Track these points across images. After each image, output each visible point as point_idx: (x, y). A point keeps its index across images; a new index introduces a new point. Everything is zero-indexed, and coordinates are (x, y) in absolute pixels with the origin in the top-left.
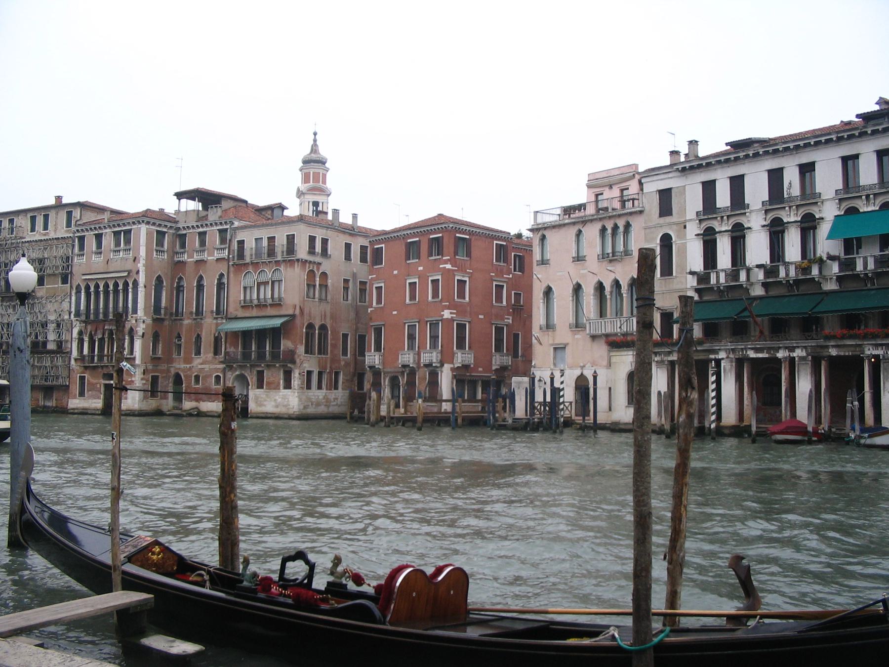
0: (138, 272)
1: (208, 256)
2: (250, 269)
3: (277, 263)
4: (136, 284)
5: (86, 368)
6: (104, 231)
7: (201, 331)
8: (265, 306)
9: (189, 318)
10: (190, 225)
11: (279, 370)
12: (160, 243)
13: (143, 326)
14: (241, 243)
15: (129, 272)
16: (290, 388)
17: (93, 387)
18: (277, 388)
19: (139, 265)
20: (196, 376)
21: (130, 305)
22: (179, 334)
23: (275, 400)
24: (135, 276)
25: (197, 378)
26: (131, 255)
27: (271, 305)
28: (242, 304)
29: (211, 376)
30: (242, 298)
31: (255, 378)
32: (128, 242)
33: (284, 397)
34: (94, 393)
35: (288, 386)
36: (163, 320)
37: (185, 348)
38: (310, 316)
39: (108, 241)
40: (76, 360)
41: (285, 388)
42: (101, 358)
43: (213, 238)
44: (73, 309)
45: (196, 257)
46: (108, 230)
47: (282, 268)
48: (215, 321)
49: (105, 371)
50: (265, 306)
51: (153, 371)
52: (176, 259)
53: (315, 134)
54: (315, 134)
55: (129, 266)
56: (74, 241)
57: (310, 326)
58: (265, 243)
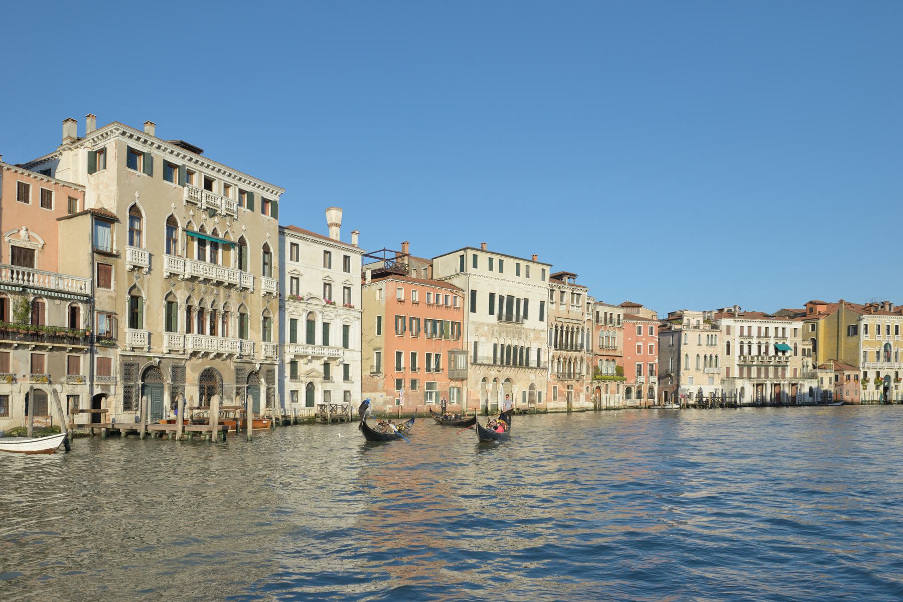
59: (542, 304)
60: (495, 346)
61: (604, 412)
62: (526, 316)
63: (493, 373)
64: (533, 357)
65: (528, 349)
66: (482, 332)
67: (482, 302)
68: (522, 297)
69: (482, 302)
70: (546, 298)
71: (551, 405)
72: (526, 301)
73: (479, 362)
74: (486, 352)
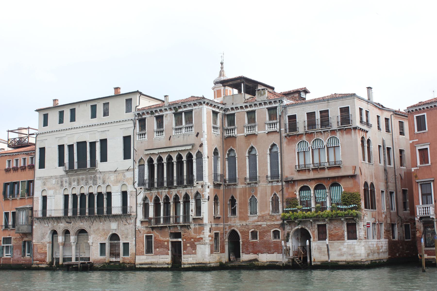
0: (201, 145)
1: (259, 130)
2: (304, 138)
3: (333, 132)
4: (200, 155)
5: (153, 228)
6: (164, 113)
7: (256, 194)
8: (323, 169)
9: (242, 183)
10: (239, 106)
11: (342, 222)
12: (215, 122)
13: (208, 190)
14: (292, 118)
15: (193, 145)
16: (355, 238)
17: (160, 244)
18: (341, 238)
19: (202, 139)
20: (252, 232)
21: (195, 173)
22: (233, 197)
23: (340, 250)
24: (199, 149)
25: (254, 234)
26: (194, 131)
27: (329, 168)
28: (298, 169)
30: (297, 164)
31: (316, 232)
32: (189, 120)
33: (350, 247)
34: (161, 250)
35: (352, 235)
36: (220, 185)
37: (240, 208)
38: (365, 176)
39: (169, 120)
40: (142, 222)
41: (349, 238)
42: (167, 219)
43: (262, 114)
44: (137, 180)
45: (246, 132)
46: (169, 112)
47: (338, 135)
48: (270, 185)
49: (173, 230)
50: (323, 169)
51: (217, 229)
52: (226, 135)
53: (222, 64)
54: (222, 64)
55: (192, 139)
56: (135, 124)
57: (366, 184)
58: (318, 116)
59: (127, 140)
60: (66, 197)
63: (61, 226)
64: (117, 202)
67: (52, 156)
68: (97, 138)
69: (52, 156)
70: (129, 129)
71: (142, 259)
73: (48, 215)
74: (55, 207)
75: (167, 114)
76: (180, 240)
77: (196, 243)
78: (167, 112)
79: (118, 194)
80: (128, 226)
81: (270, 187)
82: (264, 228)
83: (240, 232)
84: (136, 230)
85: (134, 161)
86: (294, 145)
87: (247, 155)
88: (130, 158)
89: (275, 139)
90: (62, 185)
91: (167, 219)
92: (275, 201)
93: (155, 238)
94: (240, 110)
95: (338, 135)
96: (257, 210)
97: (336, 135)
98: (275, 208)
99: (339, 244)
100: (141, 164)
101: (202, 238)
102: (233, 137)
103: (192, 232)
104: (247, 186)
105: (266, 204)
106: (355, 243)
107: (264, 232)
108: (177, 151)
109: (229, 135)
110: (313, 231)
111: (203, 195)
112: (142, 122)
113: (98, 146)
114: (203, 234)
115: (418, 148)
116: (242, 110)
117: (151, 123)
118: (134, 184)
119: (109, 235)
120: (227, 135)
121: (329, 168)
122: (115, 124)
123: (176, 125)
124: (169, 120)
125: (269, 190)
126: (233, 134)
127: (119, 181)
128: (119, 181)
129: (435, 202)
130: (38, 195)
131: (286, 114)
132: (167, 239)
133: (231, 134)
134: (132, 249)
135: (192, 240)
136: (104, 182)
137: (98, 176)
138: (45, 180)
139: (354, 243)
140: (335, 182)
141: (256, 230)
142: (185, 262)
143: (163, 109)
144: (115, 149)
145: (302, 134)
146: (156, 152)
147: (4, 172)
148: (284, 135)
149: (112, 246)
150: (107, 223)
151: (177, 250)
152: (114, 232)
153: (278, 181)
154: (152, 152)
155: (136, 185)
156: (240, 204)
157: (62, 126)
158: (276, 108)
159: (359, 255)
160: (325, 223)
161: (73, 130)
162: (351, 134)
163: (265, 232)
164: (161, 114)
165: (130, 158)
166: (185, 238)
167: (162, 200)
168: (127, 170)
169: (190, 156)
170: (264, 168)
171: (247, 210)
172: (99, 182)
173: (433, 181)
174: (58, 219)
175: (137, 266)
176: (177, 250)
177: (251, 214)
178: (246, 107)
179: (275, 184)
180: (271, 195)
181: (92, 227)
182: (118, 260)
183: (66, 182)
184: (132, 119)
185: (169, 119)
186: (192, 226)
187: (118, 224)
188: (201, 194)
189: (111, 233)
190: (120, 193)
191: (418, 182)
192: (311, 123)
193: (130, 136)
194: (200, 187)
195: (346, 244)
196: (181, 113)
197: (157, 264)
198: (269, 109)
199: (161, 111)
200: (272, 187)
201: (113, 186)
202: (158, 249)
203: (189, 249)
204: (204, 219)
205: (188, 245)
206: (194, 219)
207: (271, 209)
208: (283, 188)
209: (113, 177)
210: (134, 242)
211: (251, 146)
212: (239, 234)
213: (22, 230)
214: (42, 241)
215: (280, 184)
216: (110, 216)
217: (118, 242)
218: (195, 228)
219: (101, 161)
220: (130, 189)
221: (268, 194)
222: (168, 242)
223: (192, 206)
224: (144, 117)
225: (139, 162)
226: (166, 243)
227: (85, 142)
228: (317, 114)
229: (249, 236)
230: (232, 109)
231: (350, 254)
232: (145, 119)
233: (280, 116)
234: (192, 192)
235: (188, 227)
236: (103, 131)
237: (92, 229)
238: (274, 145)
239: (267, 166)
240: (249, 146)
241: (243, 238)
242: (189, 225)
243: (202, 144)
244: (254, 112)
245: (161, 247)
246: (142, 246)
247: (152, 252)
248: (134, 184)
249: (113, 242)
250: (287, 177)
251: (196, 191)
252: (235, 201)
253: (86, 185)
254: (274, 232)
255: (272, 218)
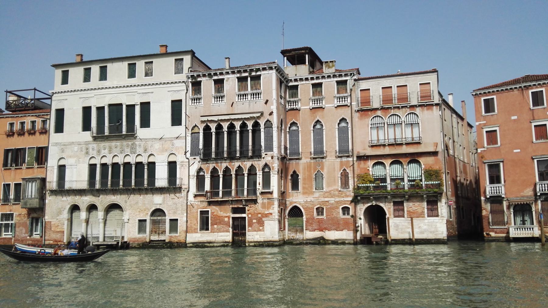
0: (271, 114)
3: (413, 107)
4: (269, 124)
6: (225, 77)
7: (322, 168)
8: (401, 144)
9: (306, 158)
20: (317, 209)
22: (294, 172)
23: (420, 227)
25: (320, 211)
27: (407, 144)
29: (338, 208)
37: (304, 184)
39: (231, 83)
44: (189, 149)
45: (311, 105)
46: (231, 76)
48: (339, 160)
50: (401, 144)
58: (395, 91)
59: (176, 106)
60: (92, 168)
61: (394, 249)
62: (146, 123)
63: (84, 201)
65: (152, 165)
66: (73, 153)
67: (73, 120)
68: (136, 100)
69: (73, 120)
70: (182, 92)
72: (146, 107)
74: (77, 177)
75: (228, 78)
76: (244, 215)
77: (264, 219)
78: (228, 76)
79: (164, 164)
80: (176, 200)
81: (339, 163)
82: (332, 204)
83: (304, 208)
84: (187, 205)
85: (186, 128)
86: (367, 120)
87: (312, 129)
88: (180, 124)
89: (345, 113)
90: (87, 153)
91: (227, 193)
92: (345, 176)
93: (212, 213)
94: (304, 82)
95: (418, 111)
96: (324, 185)
97: (415, 111)
98: (345, 184)
99: (419, 221)
100: (193, 131)
101: (271, 214)
102: (297, 109)
103: (258, 207)
104: (313, 161)
105: (335, 181)
106: (437, 221)
107: (331, 208)
108: (242, 119)
109: (292, 107)
110: (388, 208)
111: (273, 167)
112: (197, 85)
113: (138, 110)
114: (273, 209)
115: (485, 130)
116: (307, 82)
117: (208, 85)
118: (186, 153)
119: (151, 210)
120: (290, 107)
121: (407, 144)
122: (161, 86)
123: (239, 90)
124: (231, 83)
125: (337, 166)
126: (297, 106)
127: (166, 150)
128: (166, 150)
129: (505, 182)
130: (52, 162)
131: (358, 88)
132: (228, 214)
133: (294, 106)
134: (181, 225)
135: (260, 215)
136: (145, 151)
137: (137, 143)
138: (63, 146)
139: (435, 221)
140: (414, 158)
141: (322, 206)
142: (250, 240)
143: (224, 72)
144: (161, 114)
145: (376, 109)
146: (215, 118)
147: (5, 136)
148: (355, 108)
149: (154, 222)
150: (149, 197)
151: (239, 228)
152: (158, 207)
153: (348, 157)
154: (210, 118)
155: (188, 154)
156: (304, 179)
157: (87, 85)
158: (346, 81)
159: (440, 232)
160: (402, 200)
161: (103, 90)
162: (432, 110)
163: (333, 208)
164: (221, 77)
165: (180, 124)
166: (250, 214)
167: (222, 172)
168: (177, 138)
169: (256, 125)
170: (331, 143)
171: (312, 185)
172: (139, 150)
173: (503, 162)
174: (80, 192)
175: (188, 245)
176: (239, 228)
177: (316, 189)
178: (312, 79)
179: (344, 159)
180: (340, 170)
181: (128, 201)
182: (162, 238)
183: (93, 149)
184: (183, 82)
185: (231, 83)
186: (260, 201)
187: (164, 198)
188: (271, 166)
189: (154, 209)
190: (167, 164)
191: (485, 163)
192: (387, 99)
193: (181, 101)
194: (270, 158)
195: (426, 221)
196: (245, 78)
197: (214, 242)
198: (338, 83)
199: (221, 74)
200: (341, 162)
201: (158, 155)
202: (215, 226)
203: (256, 226)
204: (274, 193)
205: (254, 221)
206: (262, 193)
207: (340, 185)
208: (354, 164)
209: (157, 145)
210: (185, 219)
211: (317, 119)
212: (303, 210)
213: (30, 205)
214: (58, 218)
215: (351, 159)
216: (153, 189)
217: (163, 218)
218: (263, 203)
219: (141, 127)
220: (180, 158)
221: (336, 169)
222: (229, 217)
223: (259, 179)
224: (199, 79)
225: (192, 129)
226: (226, 219)
227: (121, 105)
228: (394, 89)
229: (313, 213)
230: (296, 80)
231: (431, 232)
232: (200, 82)
233: (351, 90)
234: (259, 164)
235: (255, 201)
236: (145, 93)
237: (128, 204)
238: (343, 120)
239: (336, 140)
240: (314, 119)
241: (307, 215)
242: (256, 200)
243: (272, 112)
244: (320, 85)
245: (220, 223)
246: (196, 222)
247: (207, 229)
248: (186, 153)
249: (155, 218)
250: (358, 152)
251: (264, 163)
252: (298, 176)
253: (121, 153)
254: (342, 208)
255: (342, 194)
